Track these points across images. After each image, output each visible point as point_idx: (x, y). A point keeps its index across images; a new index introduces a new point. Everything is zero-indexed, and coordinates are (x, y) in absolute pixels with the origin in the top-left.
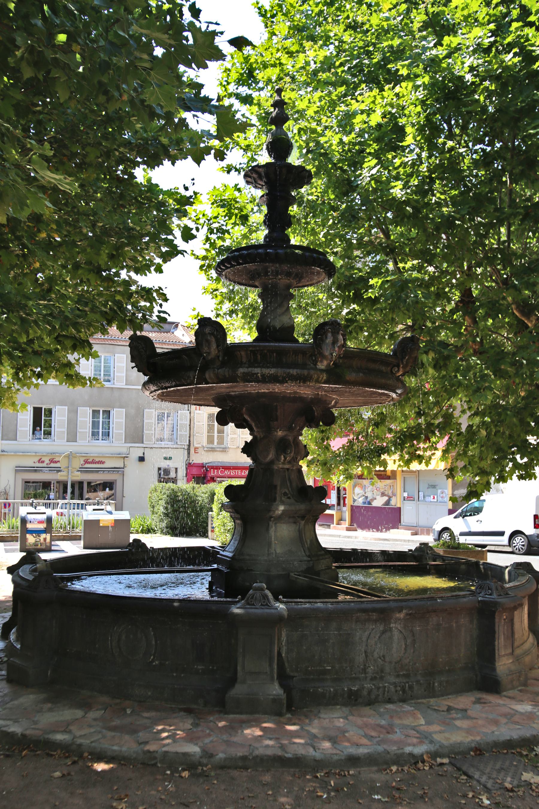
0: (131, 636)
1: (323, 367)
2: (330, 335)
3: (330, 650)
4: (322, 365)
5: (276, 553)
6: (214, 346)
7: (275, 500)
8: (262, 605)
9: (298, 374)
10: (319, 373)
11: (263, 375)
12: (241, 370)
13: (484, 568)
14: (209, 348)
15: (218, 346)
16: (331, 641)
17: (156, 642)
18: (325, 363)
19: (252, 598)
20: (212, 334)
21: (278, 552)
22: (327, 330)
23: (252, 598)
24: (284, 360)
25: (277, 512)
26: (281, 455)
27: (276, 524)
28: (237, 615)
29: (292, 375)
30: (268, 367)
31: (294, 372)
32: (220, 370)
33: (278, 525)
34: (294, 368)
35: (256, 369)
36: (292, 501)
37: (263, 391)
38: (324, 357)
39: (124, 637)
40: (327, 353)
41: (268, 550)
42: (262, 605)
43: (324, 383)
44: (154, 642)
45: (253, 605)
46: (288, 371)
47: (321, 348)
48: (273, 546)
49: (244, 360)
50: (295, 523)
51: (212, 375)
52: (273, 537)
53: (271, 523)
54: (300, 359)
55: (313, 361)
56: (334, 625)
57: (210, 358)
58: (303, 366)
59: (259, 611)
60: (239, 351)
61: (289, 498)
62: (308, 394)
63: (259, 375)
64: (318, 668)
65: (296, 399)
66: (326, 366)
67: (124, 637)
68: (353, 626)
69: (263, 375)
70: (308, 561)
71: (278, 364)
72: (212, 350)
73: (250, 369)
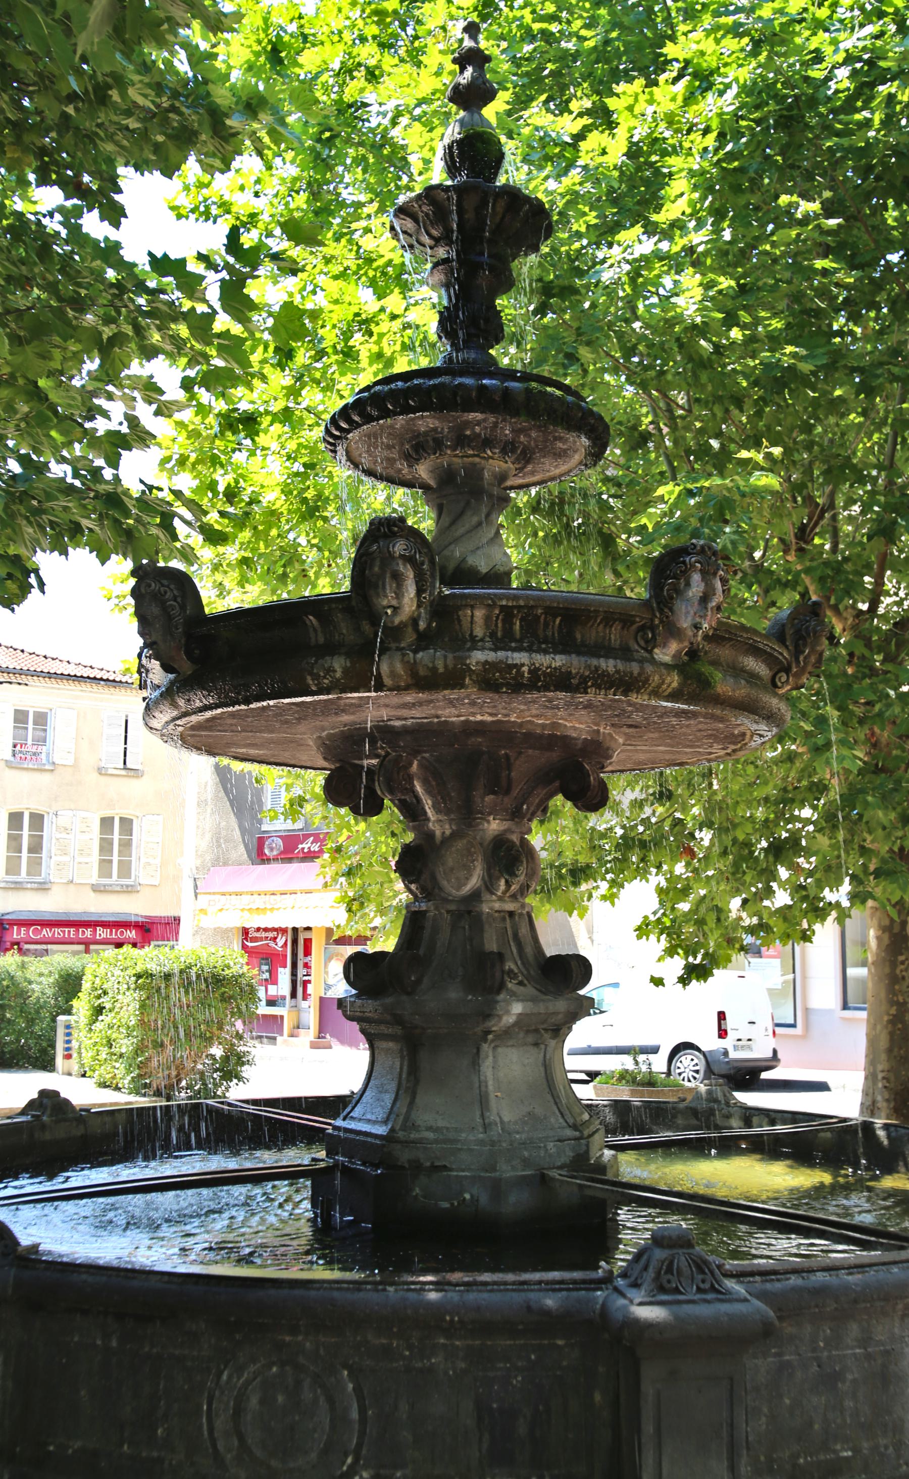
0: (280, 1399)
1: (667, 659)
2: (696, 577)
3: (849, 1404)
4: (665, 654)
5: (502, 1122)
6: (411, 590)
7: (501, 987)
8: (699, 1290)
9: (618, 672)
10: (664, 671)
11: (534, 671)
12: (478, 657)
13: (889, 1136)
14: (399, 595)
15: (419, 592)
16: (849, 1377)
17: (362, 1411)
18: (674, 646)
19: (669, 1270)
20: (410, 560)
21: (506, 1119)
22: (692, 566)
23: (669, 1270)
24: (578, 636)
25: (505, 1018)
26: (498, 879)
27: (495, 1048)
28: (649, 1326)
29: (605, 674)
30: (545, 652)
31: (609, 665)
32: (420, 655)
33: (500, 1050)
34: (607, 657)
35: (516, 655)
36: (530, 990)
37: (479, 718)
38: (674, 632)
39: (254, 1402)
40: (685, 623)
41: (482, 1115)
42: (699, 1290)
43: (668, 698)
44: (355, 1415)
45: (677, 1291)
46: (594, 662)
47: (671, 609)
48: (493, 1103)
49: (479, 632)
50: (536, 1044)
51: (399, 668)
52: (490, 1083)
53: (485, 1047)
54: (615, 635)
55: (647, 642)
56: (854, 1329)
57: (397, 621)
58: (625, 653)
59: (706, 1311)
60: (472, 607)
61: (521, 983)
62: (581, 730)
63: (525, 669)
64: (822, 1457)
65: (555, 741)
66: (674, 656)
67: (254, 1402)
68: (896, 1330)
69: (534, 671)
70: (575, 1139)
71: (565, 645)
72: (406, 600)
73: (501, 654)
